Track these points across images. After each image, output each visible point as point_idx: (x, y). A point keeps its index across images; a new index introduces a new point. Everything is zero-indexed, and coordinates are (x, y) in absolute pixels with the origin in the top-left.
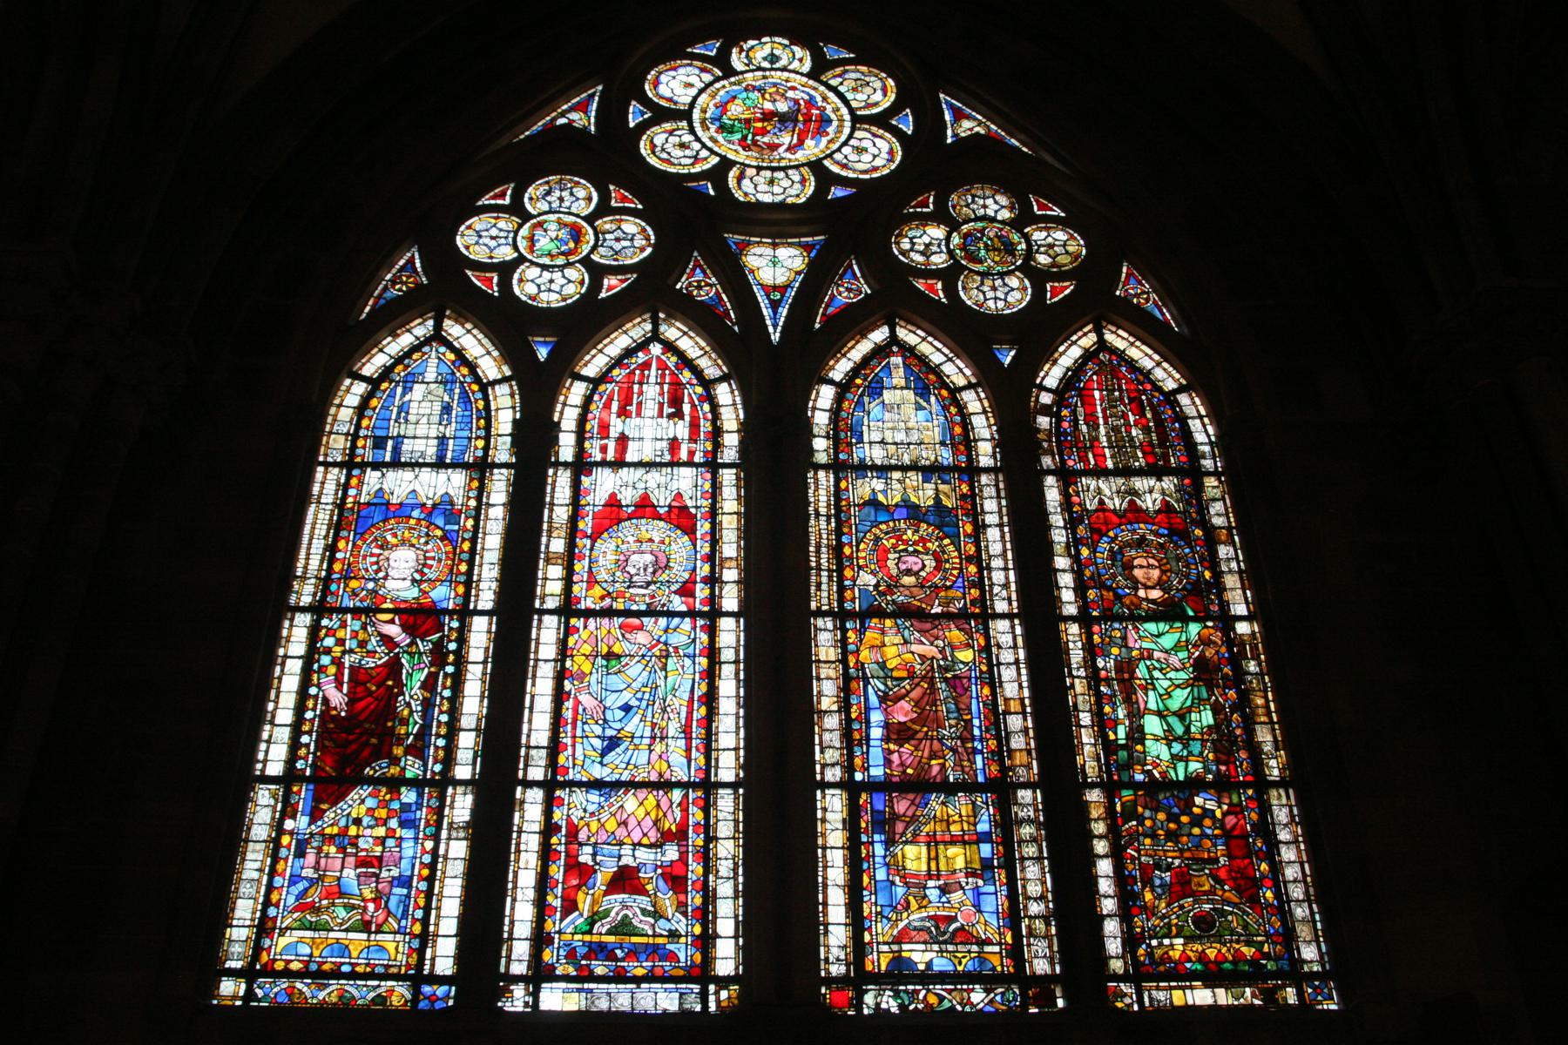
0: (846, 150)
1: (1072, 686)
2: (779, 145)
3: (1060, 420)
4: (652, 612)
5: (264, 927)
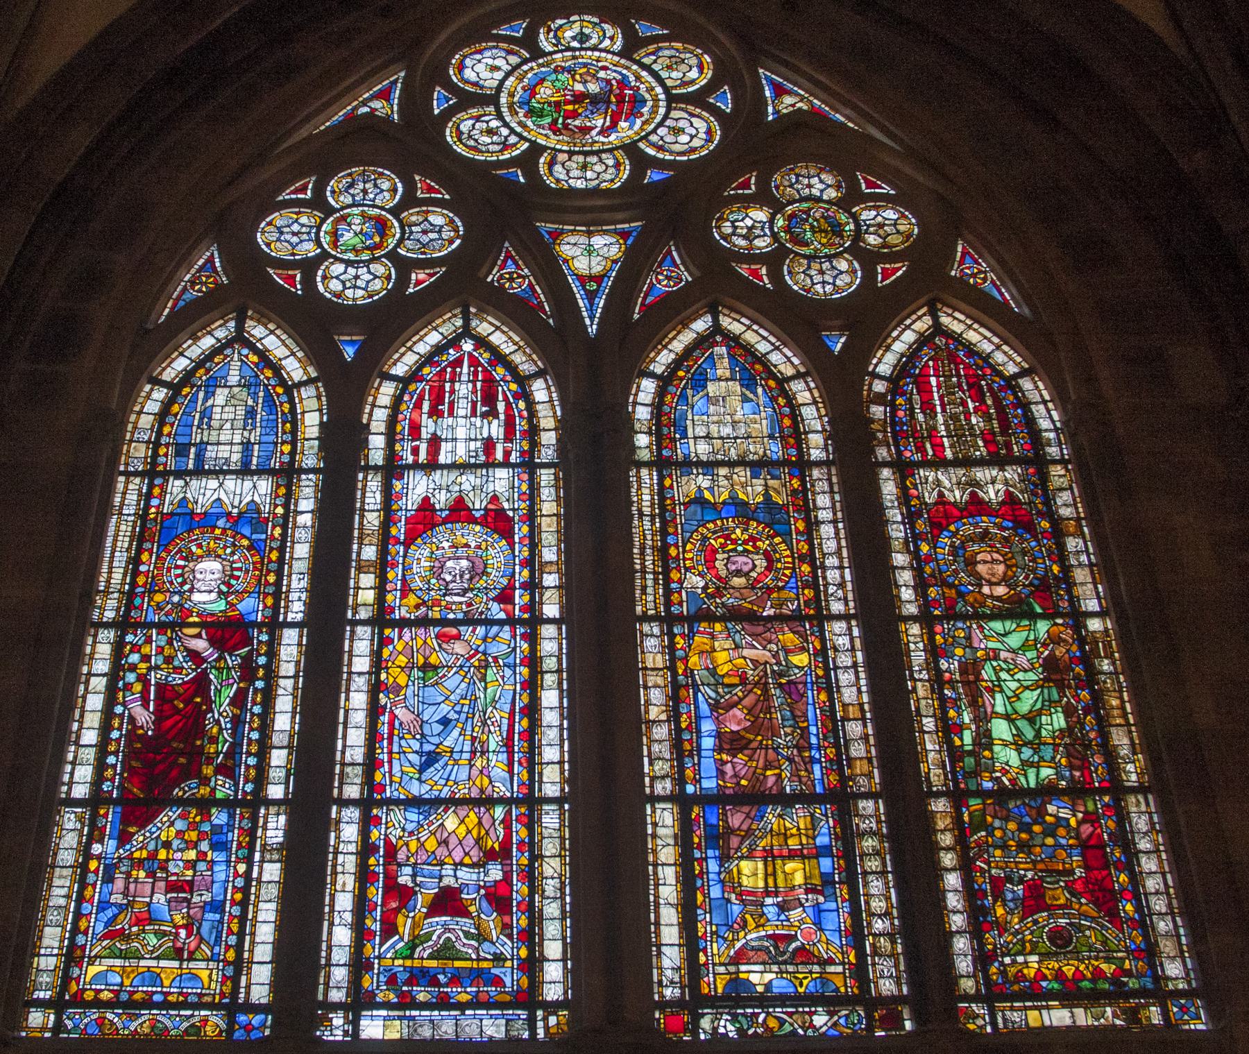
0: (662, 131)
1: (914, 689)
2: (591, 129)
3: (894, 409)
4: (469, 621)
5: (73, 956)
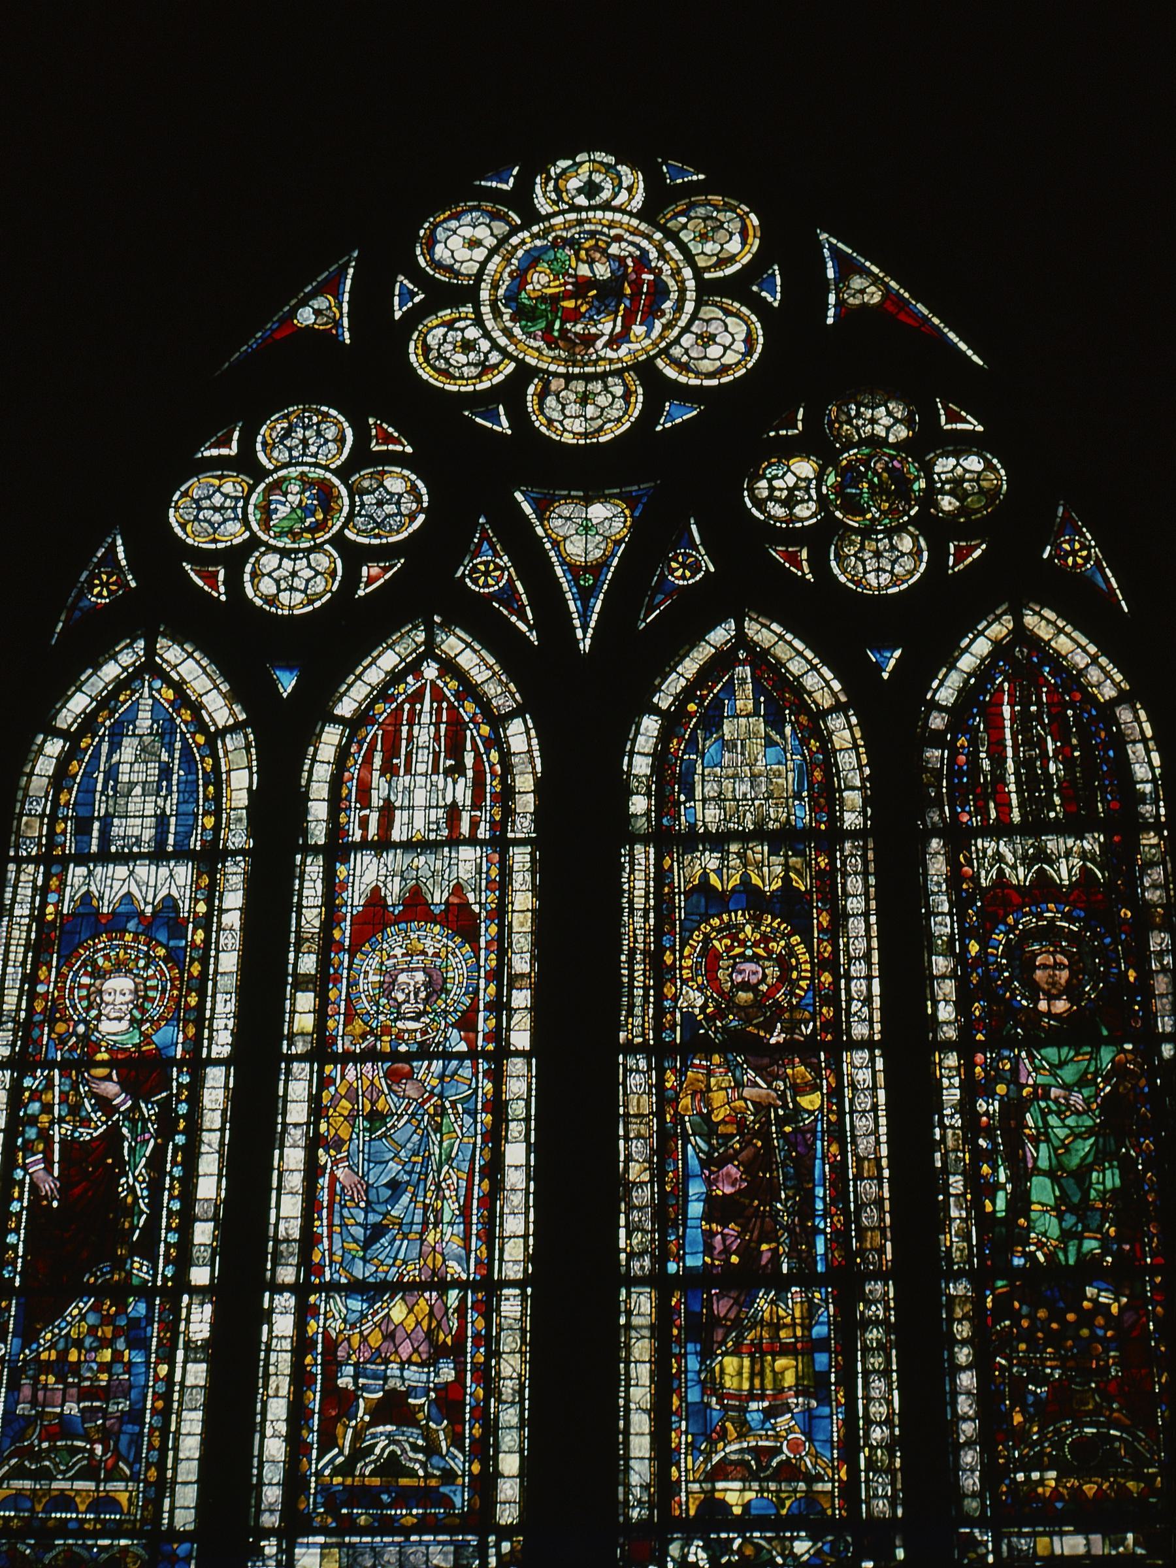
0: (687, 340)
1: (944, 1136)
2: (597, 337)
3: (954, 752)
4: (425, 1053)
